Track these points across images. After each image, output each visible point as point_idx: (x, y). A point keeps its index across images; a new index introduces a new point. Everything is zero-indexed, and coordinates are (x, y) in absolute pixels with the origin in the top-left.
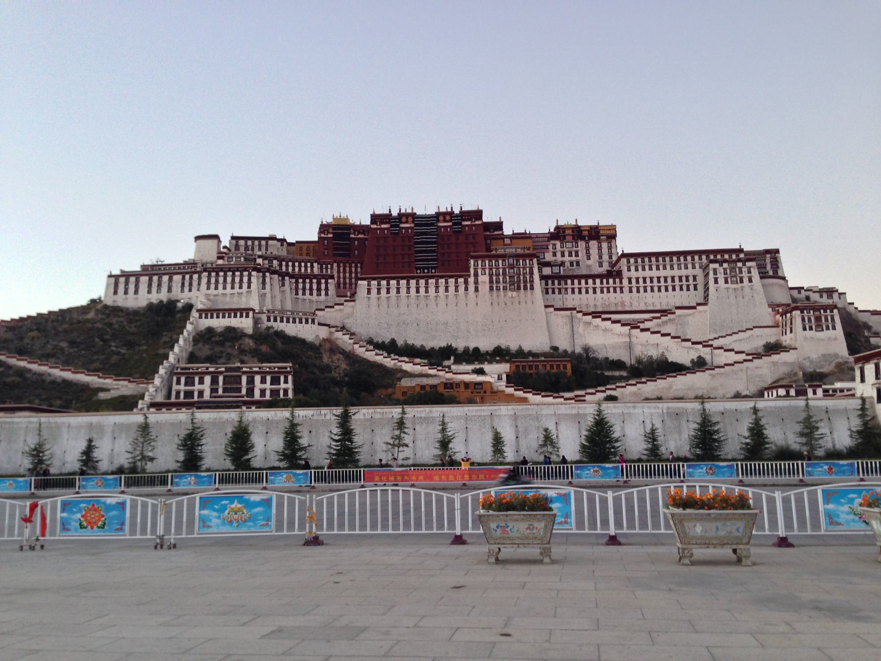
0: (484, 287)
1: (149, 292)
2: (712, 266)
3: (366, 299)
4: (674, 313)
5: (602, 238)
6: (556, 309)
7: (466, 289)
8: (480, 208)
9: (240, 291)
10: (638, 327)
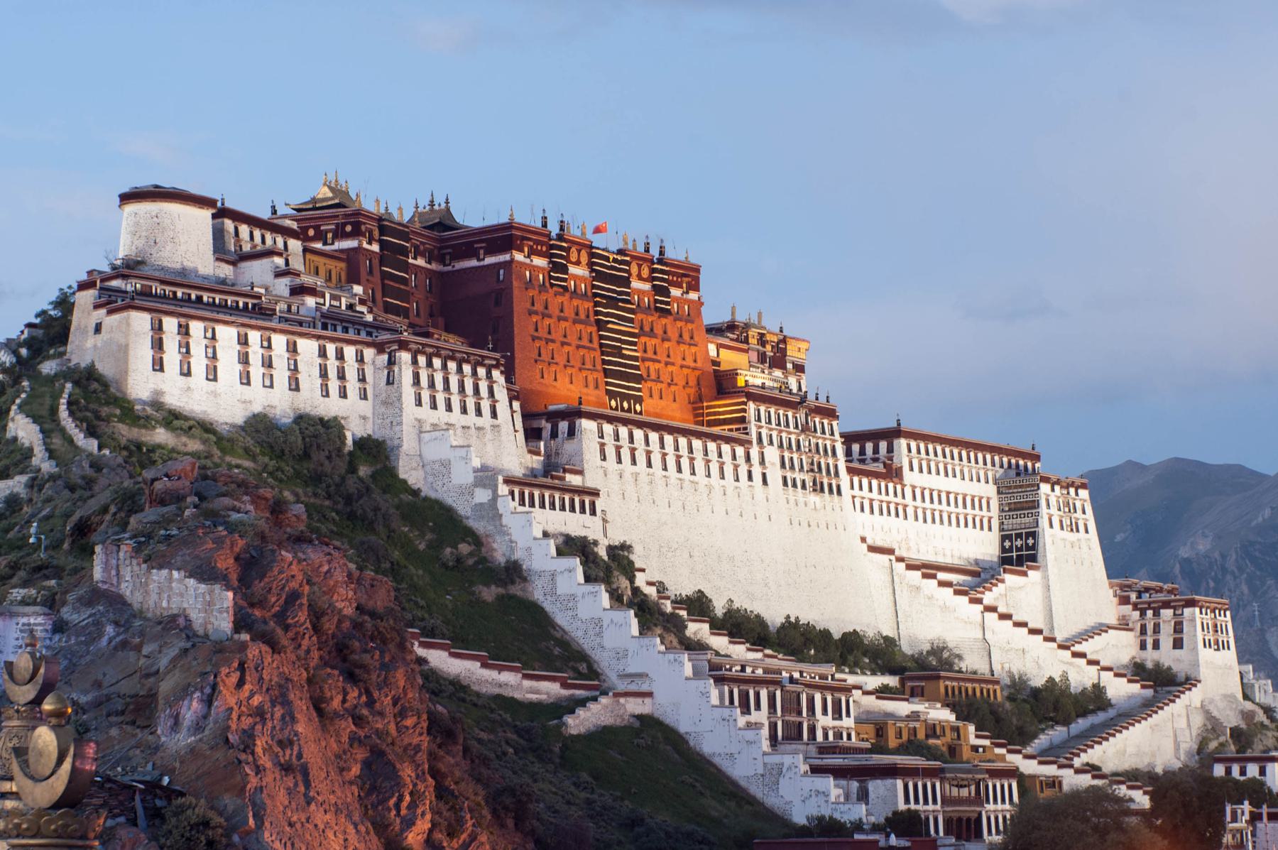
0: (775, 474)
1: (246, 379)
2: (1045, 488)
3: (601, 472)
4: (1003, 581)
5: (789, 366)
6: (873, 549)
7: (750, 478)
8: (693, 260)
9: (479, 422)
10: (992, 609)
